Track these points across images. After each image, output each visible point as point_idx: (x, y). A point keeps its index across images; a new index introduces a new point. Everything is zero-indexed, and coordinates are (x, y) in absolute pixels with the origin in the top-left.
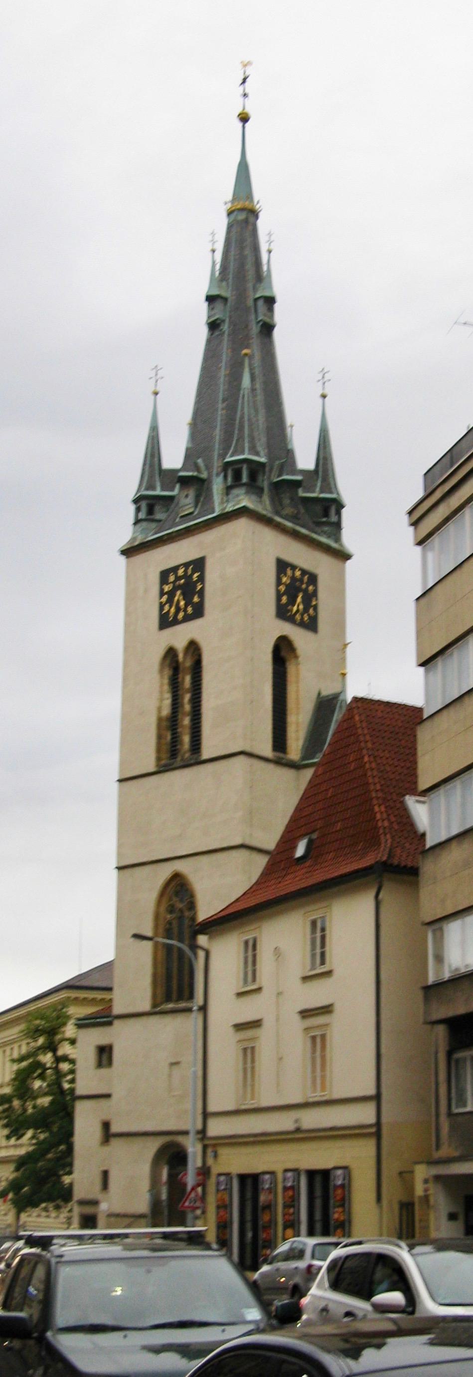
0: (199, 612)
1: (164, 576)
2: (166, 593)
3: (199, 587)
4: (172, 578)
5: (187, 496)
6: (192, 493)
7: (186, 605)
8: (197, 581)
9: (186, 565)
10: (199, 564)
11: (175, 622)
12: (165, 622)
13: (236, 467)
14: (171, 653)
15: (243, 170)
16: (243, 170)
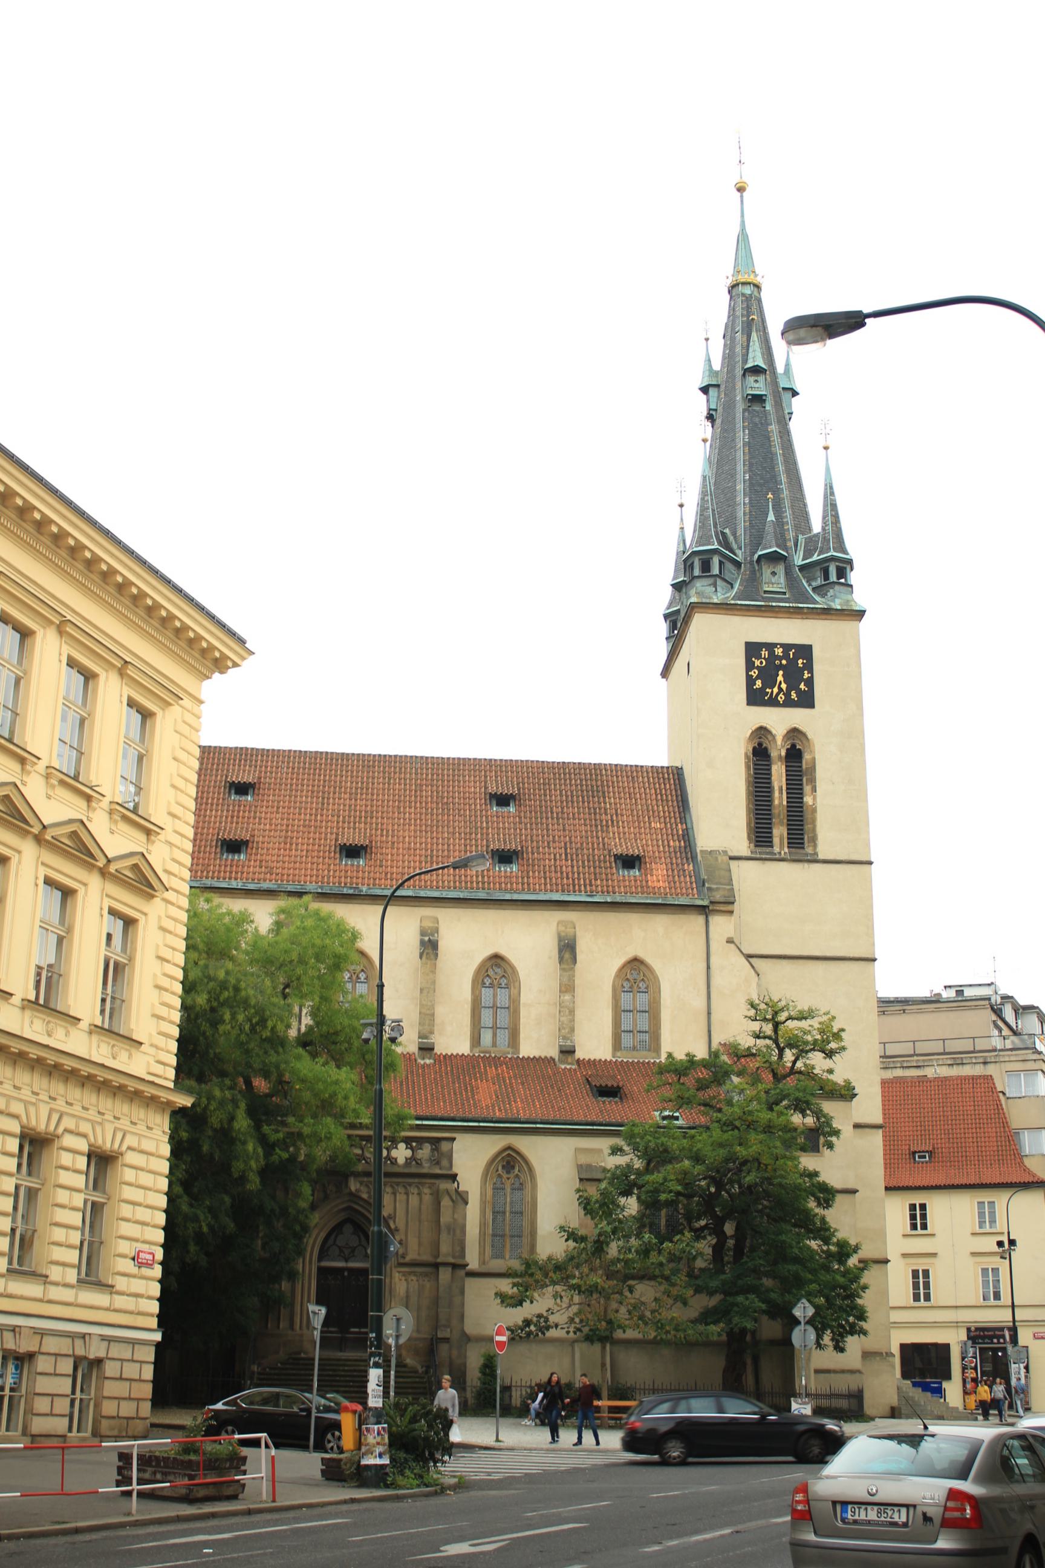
0: (807, 700)
1: (752, 649)
2: (758, 667)
3: (806, 675)
4: (764, 653)
5: (774, 574)
6: (780, 569)
7: (789, 690)
8: (803, 669)
9: (787, 647)
10: (805, 651)
11: (773, 702)
12: (755, 698)
13: (841, 565)
14: (762, 732)
15: (743, 239)
16: (743, 239)
